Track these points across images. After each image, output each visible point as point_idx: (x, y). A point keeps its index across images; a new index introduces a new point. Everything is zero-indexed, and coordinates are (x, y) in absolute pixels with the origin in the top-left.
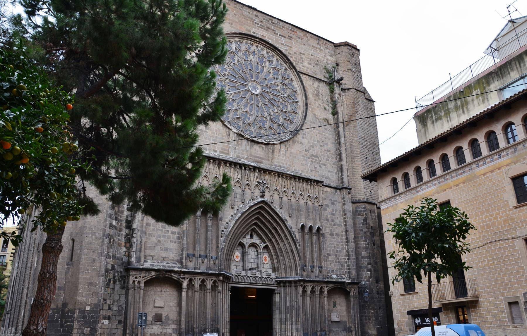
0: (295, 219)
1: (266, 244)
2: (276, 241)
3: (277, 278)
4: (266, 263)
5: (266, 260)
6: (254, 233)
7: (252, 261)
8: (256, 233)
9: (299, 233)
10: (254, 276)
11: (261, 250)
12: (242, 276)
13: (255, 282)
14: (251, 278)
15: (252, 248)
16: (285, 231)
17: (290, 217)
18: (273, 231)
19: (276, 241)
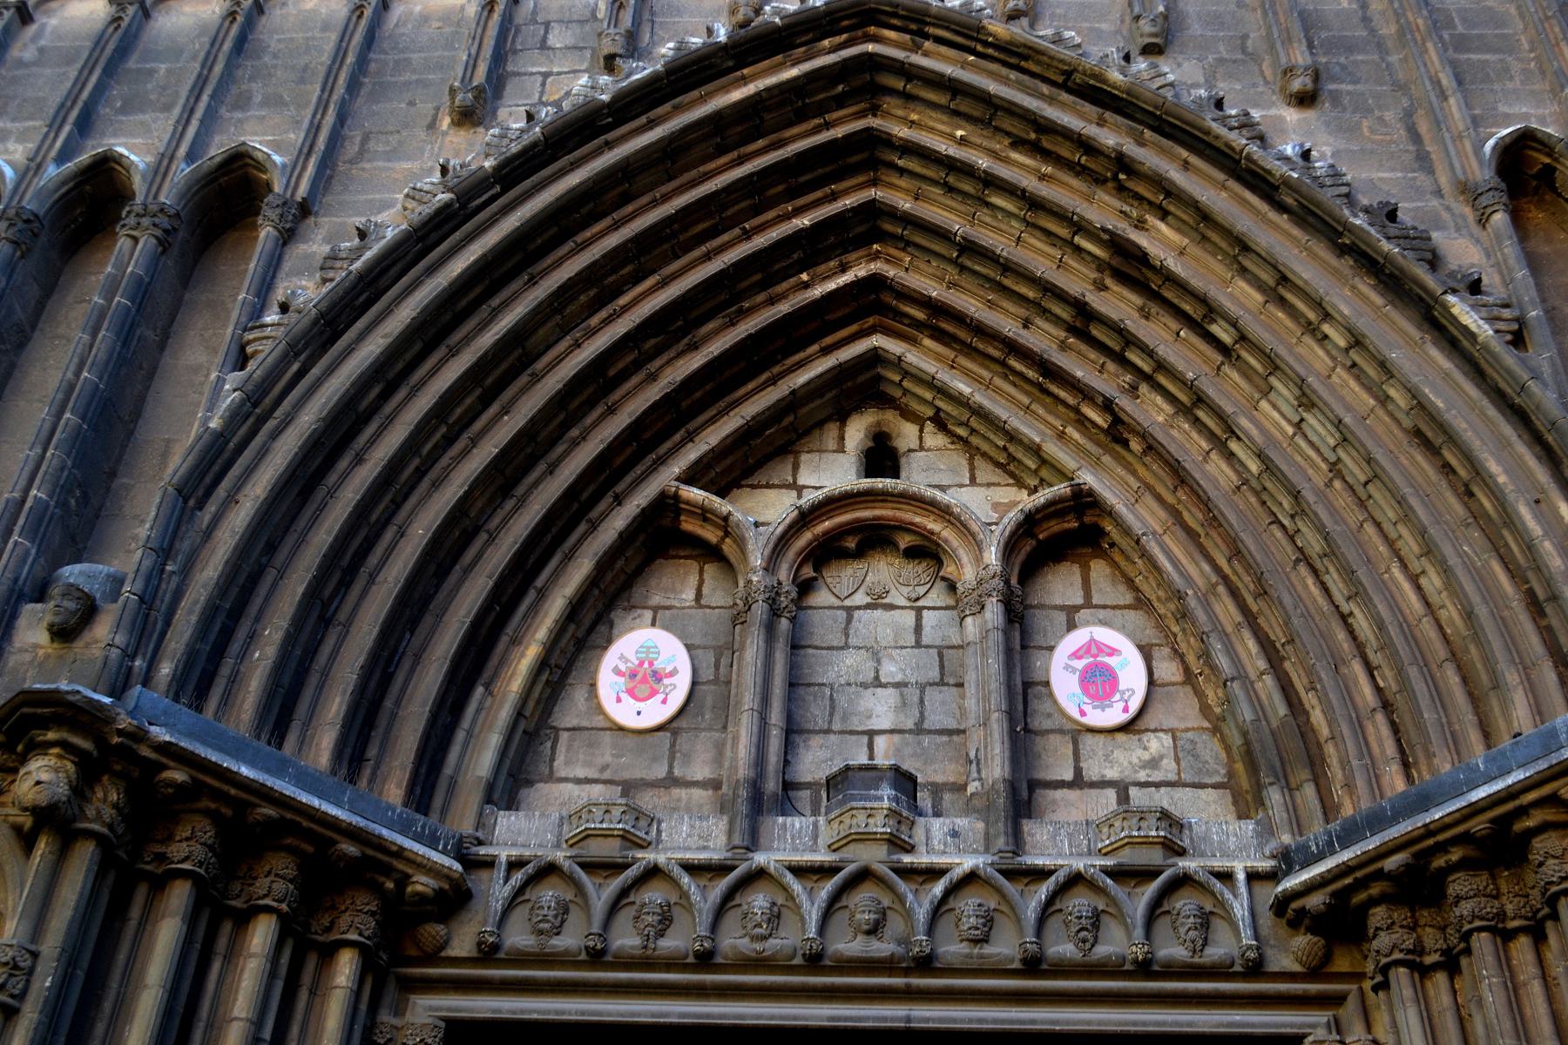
0: (1389, 116)
1: (1061, 489)
2: (1193, 404)
3: (1288, 860)
4: (1114, 715)
5: (1100, 681)
6: (906, 434)
7: (881, 710)
8: (940, 423)
9: (1483, 221)
10: (874, 856)
11: (992, 556)
12: (653, 872)
13: (882, 948)
14: (811, 901)
15: (882, 571)
16: (1244, 223)
17: (1305, 100)
18: (1118, 304)
19: (1193, 404)
